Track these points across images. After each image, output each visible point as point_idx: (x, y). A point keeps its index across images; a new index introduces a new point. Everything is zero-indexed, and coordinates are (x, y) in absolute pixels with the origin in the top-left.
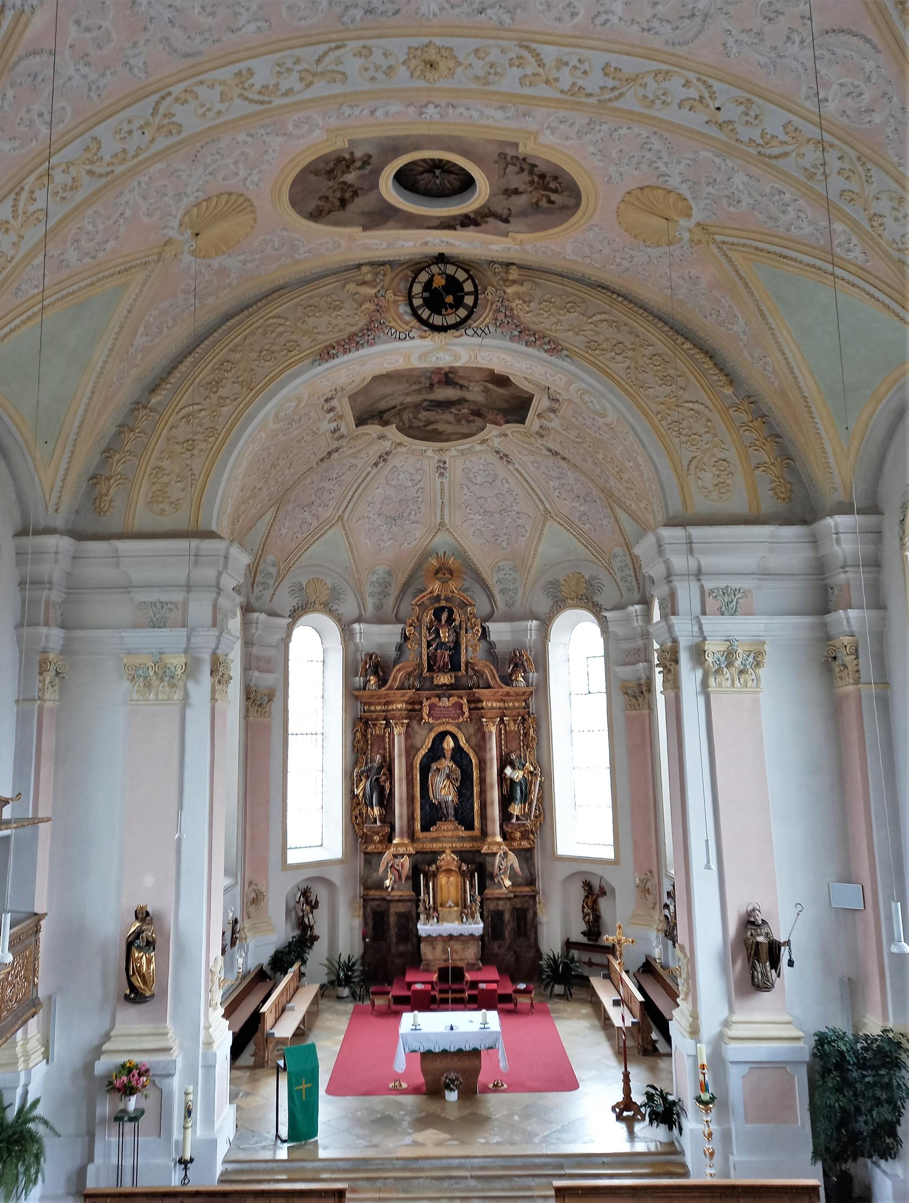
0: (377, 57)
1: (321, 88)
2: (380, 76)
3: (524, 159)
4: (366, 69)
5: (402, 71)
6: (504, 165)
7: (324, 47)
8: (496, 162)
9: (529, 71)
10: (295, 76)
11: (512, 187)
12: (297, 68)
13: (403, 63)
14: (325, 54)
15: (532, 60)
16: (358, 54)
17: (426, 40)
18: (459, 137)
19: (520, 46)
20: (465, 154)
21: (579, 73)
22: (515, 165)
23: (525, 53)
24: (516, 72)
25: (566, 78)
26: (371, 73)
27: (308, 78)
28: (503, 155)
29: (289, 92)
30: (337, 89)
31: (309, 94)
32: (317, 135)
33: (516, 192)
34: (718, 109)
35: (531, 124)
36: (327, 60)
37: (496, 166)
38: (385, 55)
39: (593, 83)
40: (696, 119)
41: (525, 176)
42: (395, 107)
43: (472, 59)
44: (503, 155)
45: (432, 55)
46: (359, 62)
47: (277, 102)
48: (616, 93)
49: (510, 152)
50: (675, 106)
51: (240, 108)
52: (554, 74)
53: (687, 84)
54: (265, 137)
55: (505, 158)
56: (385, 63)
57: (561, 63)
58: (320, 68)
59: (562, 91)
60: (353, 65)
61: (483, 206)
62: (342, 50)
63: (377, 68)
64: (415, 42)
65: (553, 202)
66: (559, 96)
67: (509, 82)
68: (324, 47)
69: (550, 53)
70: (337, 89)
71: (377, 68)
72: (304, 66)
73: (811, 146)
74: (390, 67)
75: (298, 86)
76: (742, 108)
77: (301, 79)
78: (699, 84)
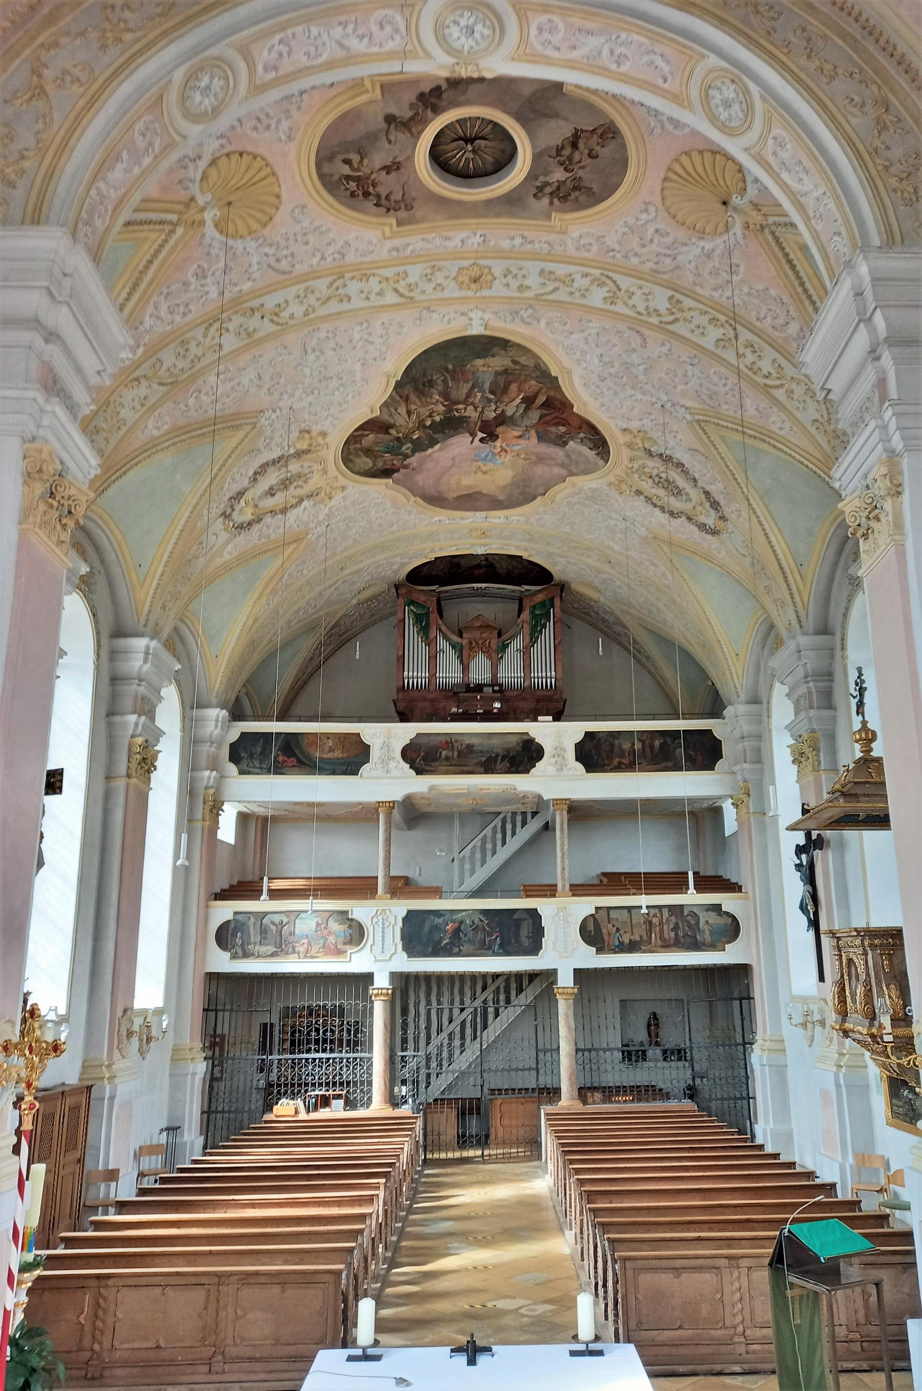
0: (514, 284)
1: (562, 270)
2: (515, 271)
3: (388, 210)
4: (524, 276)
5: (497, 271)
6: (405, 198)
7: (550, 297)
8: (414, 199)
9: (402, 283)
10: (576, 285)
11: (393, 174)
12: (573, 290)
13: (495, 279)
14: (551, 293)
15: (401, 290)
16: (528, 288)
17: (478, 294)
18: (451, 217)
19: (412, 298)
20: (443, 202)
21: (366, 291)
22: (395, 202)
23: (407, 294)
24: (411, 280)
25: (374, 284)
26: (521, 273)
27: (569, 280)
28: (409, 208)
29: (586, 275)
30: (550, 266)
31: (572, 269)
32: (575, 232)
33: (387, 169)
34: (262, 318)
35: (389, 244)
36: (551, 288)
37: (414, 194)
38: (508, 285)
39: (353, 287)
40: (270, 302)
41: (383, 191)
42: (506, 244)
43: (444, 283)
44: (409, 208)
45: (473, 286)
46: (527, 282)
47: (597, 272)
48: (335, 285)
49: (402, 214)
50: (290, 299)
51: (625, 282)
52: (384, 285)
53: (292, 316)
54: (617, 247)
55: (406, 206)
56: (509, 279)
57: (380, 294)
58: (557, 284)
59: (374, 275)
60: (533, 281)
61: (420, 132)
62: (539, 292)
63: (516, 276)
64: (486, 293)
65: (347, 162)
66: (375, 271)
67: (415, 272)
68: (550, 297)
69: (391, 298)
70: (550, 266)
71: (516, 276)
72: (569, 289)
73: (200, 354)
74: (505, 276)
75: (577, 277)
76: (251, 329)
77: (573, 281)
78: (285, 321)
